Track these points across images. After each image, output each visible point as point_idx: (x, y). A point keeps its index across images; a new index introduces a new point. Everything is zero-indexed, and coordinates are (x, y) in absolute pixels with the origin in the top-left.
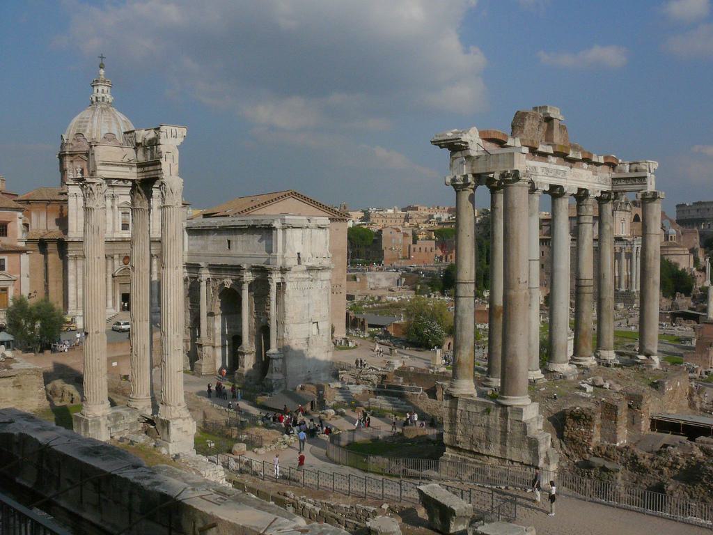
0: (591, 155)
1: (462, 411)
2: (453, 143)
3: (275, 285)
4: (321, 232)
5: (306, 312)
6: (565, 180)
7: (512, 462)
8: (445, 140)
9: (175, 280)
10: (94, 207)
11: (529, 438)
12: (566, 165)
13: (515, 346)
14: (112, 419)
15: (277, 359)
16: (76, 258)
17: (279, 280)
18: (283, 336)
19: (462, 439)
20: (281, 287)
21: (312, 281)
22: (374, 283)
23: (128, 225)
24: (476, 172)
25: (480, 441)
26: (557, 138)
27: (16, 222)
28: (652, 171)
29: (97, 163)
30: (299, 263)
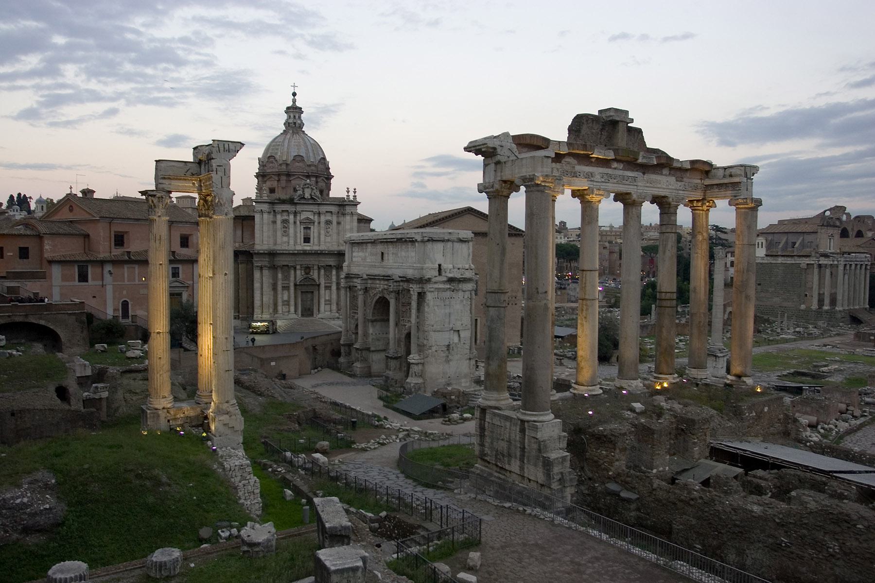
1: (489, 423)
2: (481, 149)
3: (416, 294)
4: (464, 246)
5: (447, 320)
6: (635, 187)
7: (530, 480)
8: (474, 147)
10: (155, 217)
12: (637, 171)
15: (417, 364)
16: (261, 268)
18: (423, 343)
19: (489, 452)
20: (421, 296)
21: (453, 291)
22: (574, 296)
23: (310, 238)
24: (504, 178)
25: (503, 456)
26: (622, 140)
30: (440, 274)
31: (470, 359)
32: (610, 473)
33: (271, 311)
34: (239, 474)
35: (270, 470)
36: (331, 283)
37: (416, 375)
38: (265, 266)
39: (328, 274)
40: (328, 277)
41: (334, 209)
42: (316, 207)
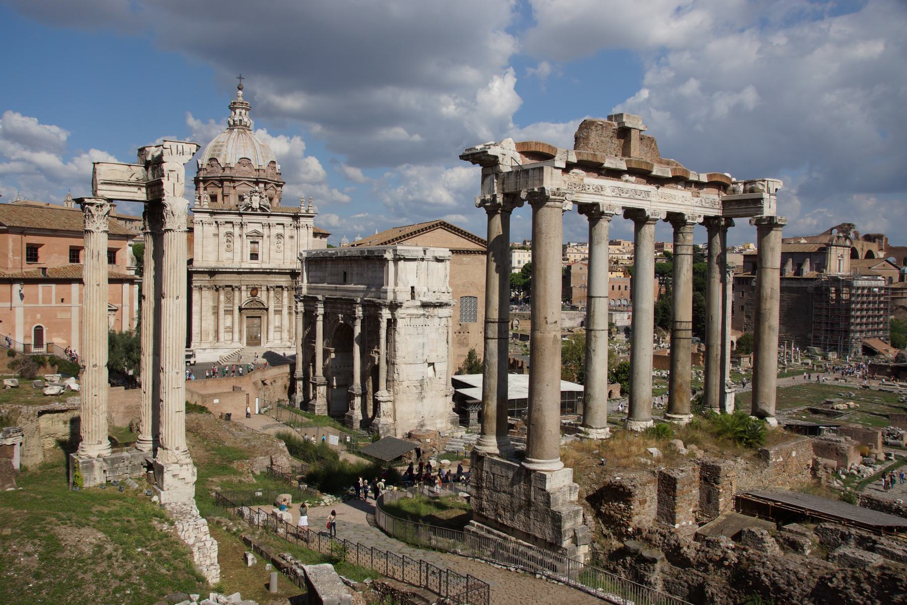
0: (687, 172)
1: (487, 472)
2: (480, 157)
4: (440, 264)
5: (420, 351)
9: (175, 311)
11: (553, 512)
13: (541, 398)
14: (109, 462)
16: (200, 288)
17: (390, 317)
20: (392, 323)
21: (427, 318)
23: (257, 255)
24: (506, 191)
25: (504, 510)
26: (637, 151)
27: (125, 248)
28: (772, 191)
29: (99, 182)
30: (413, 297)
31: (446, 396)
32: (630, 529)
33: (211, 338)
34: (193, 535)
35: (225, 528)
36: (282, 307)
37: (384, 415)
38: (205, 286)
39: (278, 296)
40: (279, 300)
41: (288, 221)
42: (265, 218)
